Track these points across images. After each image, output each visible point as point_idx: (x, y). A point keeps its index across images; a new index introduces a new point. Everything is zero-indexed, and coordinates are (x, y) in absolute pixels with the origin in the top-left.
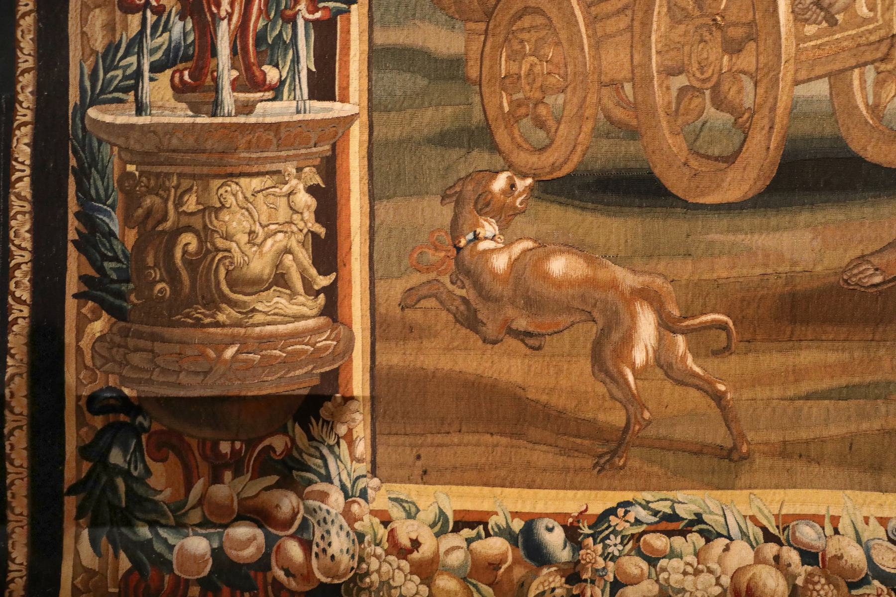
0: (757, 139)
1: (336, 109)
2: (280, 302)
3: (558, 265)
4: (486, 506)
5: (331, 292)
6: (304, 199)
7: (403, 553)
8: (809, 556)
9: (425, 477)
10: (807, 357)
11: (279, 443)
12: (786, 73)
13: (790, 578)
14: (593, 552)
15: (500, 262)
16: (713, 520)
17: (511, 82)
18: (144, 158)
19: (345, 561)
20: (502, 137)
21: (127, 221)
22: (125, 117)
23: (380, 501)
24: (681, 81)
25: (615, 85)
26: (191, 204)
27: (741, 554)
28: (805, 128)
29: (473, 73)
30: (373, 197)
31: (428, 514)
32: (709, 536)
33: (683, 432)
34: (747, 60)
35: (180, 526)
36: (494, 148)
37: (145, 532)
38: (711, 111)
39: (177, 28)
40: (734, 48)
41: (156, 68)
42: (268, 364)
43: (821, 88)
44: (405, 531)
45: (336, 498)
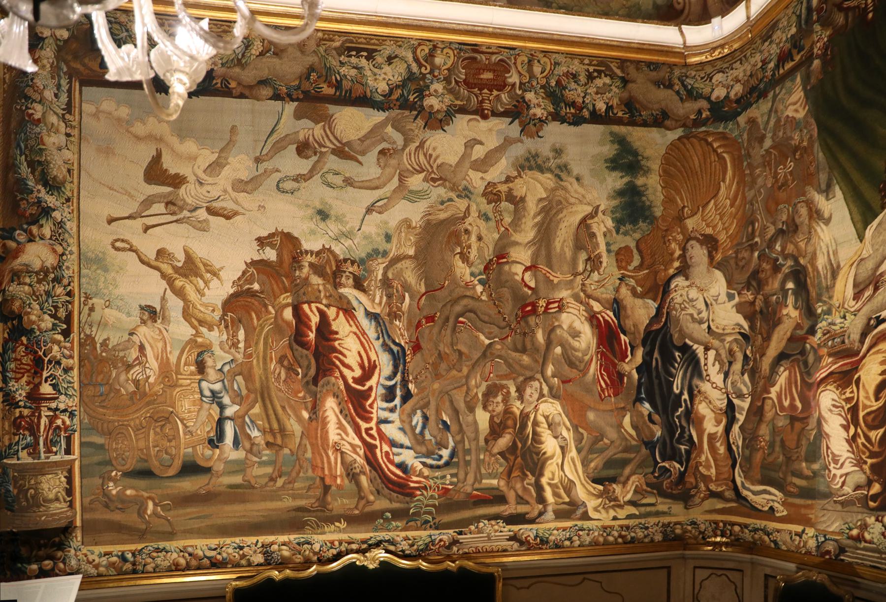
0: (176, 461)
1: (71, 457)
2: (58, 505)
3: (128, 492)
4: (112, 550)
5: (71, 501)
6: (63, 479)
7: (90, 563)
8: (190, 555)
9: (96, 544)
10: (189, 510)
11: (57, 539)
12: (182, 446)
13: (186, 560)
14: (139, 558)
15: (114, 492)
16: (168, 548)
17: (116, 449)
18: (19, 471)
19: (75, 566)
20: (114, 462)
21: (15, 487)
22: (14, 461)
23: (84, 551)
24: (158, 449)
25: (141, 450)
26: (33, 482)
27: (175, 555)
28: (187, 459)
29: (107, 447)
30: (82, 478)
31: (97, 553)
32: (167, 552)
33: (161, 529)
34: (173, 443)
35: (29, 563)
36: (112, 465)
37: (19, 565)
38: (165, 455)
39: (29, 439)
40: (170, 441)
41: (23, 449)
42: (54, 520)
43: (190, 450)
44: (91, 558)
45: (73, 551)
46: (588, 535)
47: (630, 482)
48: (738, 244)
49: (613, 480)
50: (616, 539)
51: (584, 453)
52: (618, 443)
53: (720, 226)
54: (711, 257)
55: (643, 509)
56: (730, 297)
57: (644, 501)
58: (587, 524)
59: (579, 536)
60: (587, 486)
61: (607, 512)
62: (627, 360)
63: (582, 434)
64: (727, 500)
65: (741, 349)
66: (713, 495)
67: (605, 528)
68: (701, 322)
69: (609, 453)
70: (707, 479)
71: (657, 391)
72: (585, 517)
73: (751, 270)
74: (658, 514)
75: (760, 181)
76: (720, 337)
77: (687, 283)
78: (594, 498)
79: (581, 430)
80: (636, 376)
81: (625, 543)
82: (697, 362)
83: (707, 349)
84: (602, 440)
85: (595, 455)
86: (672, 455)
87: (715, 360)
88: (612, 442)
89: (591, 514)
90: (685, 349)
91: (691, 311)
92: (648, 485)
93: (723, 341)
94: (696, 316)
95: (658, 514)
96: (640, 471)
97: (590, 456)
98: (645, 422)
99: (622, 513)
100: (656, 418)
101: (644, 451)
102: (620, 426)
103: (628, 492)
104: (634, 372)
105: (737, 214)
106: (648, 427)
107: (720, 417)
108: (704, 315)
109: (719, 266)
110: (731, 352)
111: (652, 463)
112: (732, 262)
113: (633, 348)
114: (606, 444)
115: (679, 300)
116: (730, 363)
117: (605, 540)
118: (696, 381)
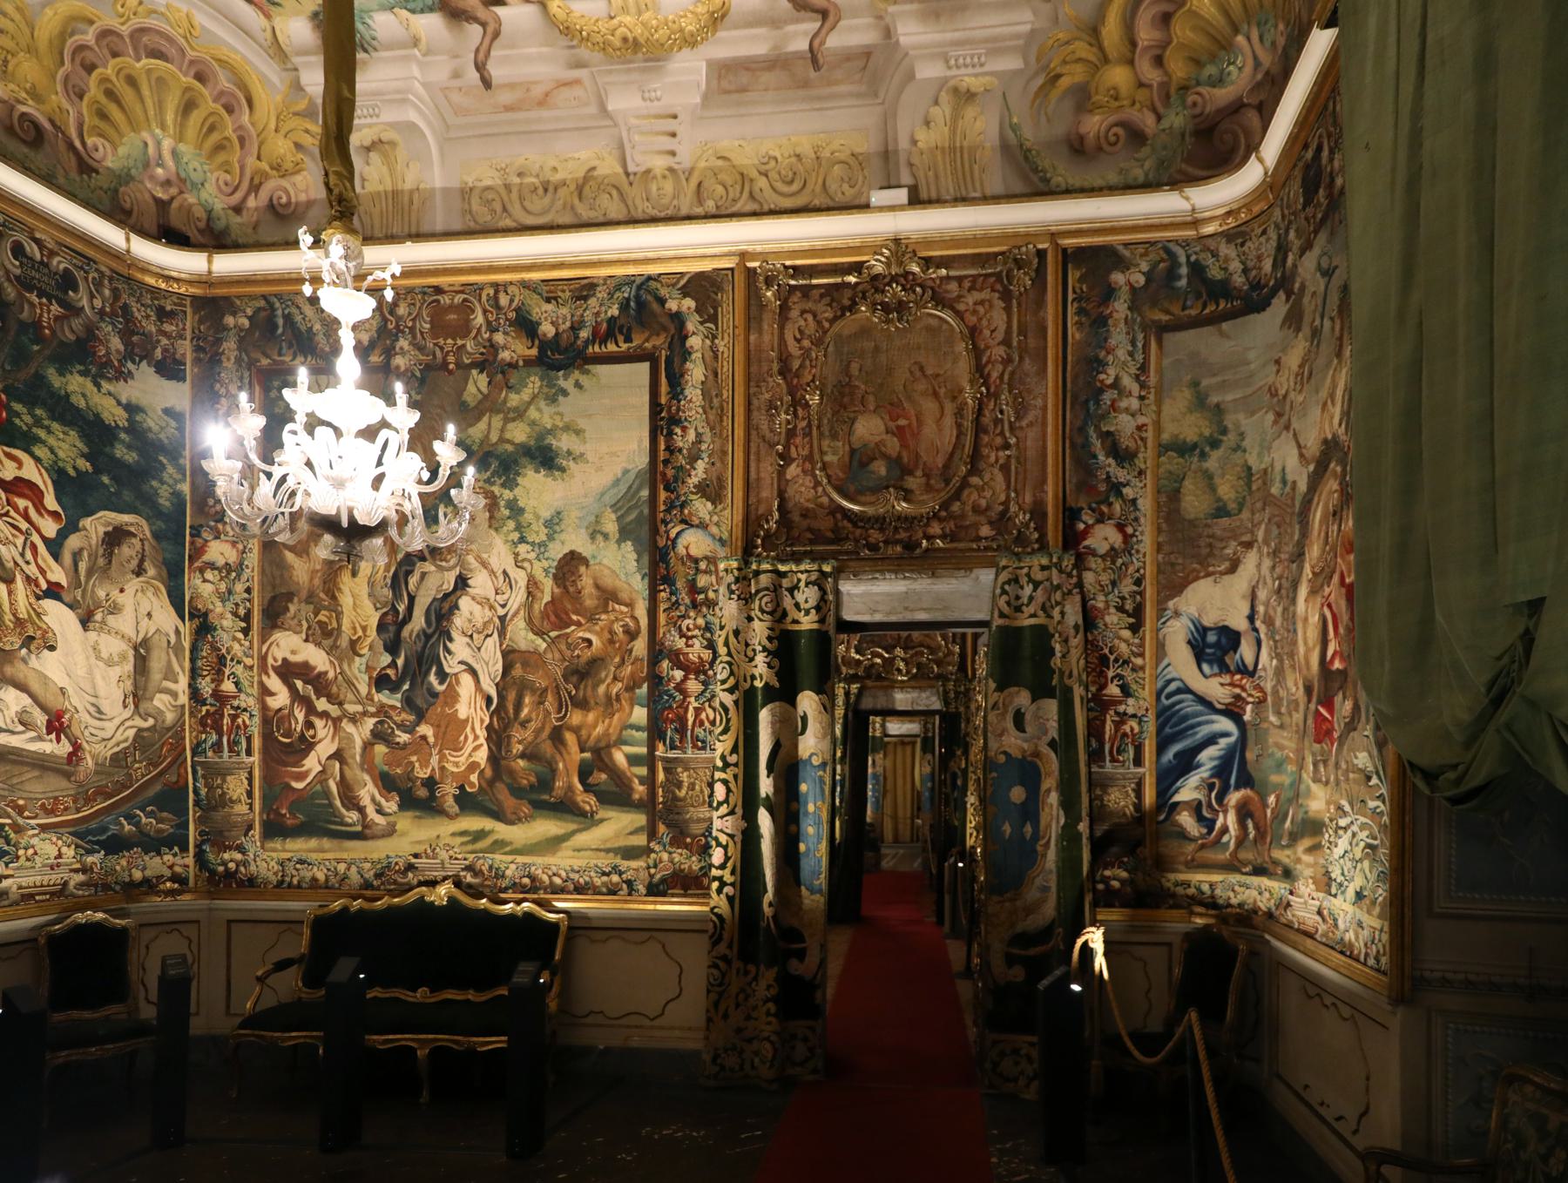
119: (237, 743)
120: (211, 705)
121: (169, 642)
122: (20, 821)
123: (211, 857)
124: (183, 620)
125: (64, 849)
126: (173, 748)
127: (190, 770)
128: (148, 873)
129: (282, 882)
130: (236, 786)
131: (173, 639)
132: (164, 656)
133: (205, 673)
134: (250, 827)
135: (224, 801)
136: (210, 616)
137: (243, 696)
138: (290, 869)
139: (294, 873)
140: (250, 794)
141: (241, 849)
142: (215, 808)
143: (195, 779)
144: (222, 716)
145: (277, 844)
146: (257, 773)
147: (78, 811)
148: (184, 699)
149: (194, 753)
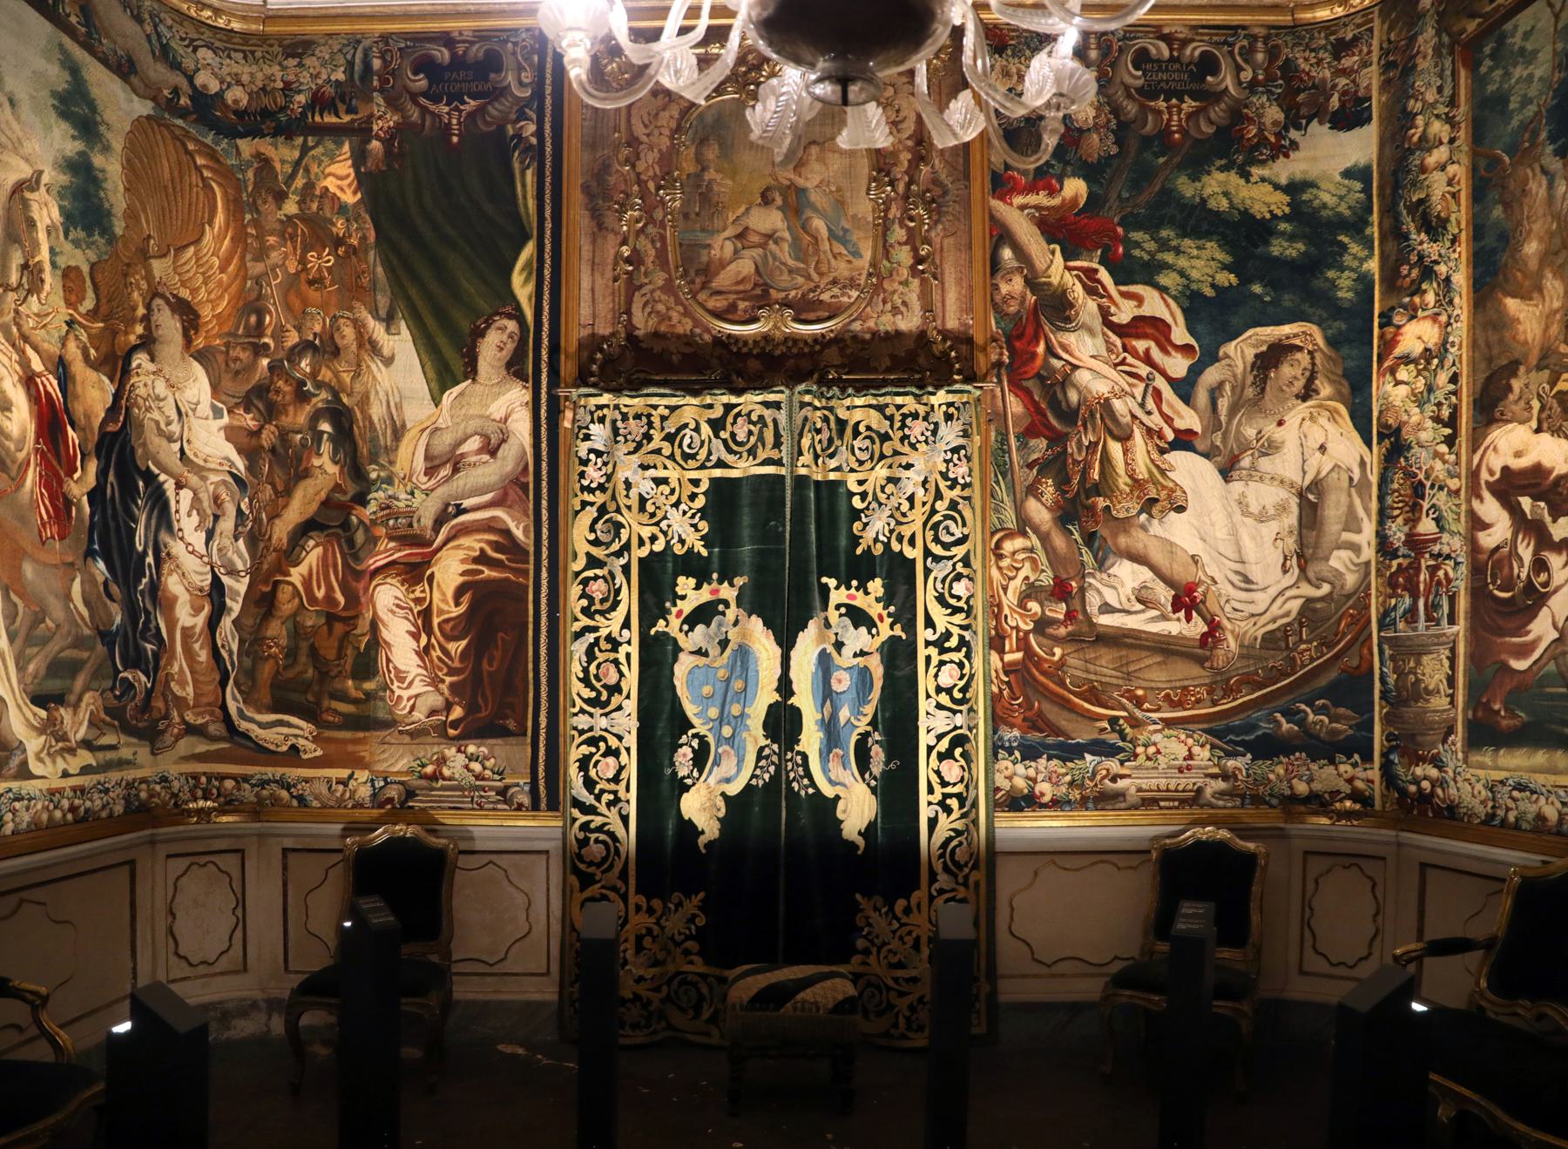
46: (28, 809)
47: (83, 705)
48: (229, 334)
49: (59, 699)
50: (64, 815)
51: (19, 642)
52: (65, 628)
53: (202, 294)
54: (188, 341)
55: (100, 755)
56: (217, 414)
57: (105, 741)
58: (29, 787)
59: (14, 812)
60: (25, 709)
61: (54, 762)
62: (76, 476)
63: (15, 605)
64: (214, 739)
65: (233, 499)
66: (191, 730)
67: (52, 792)
68: (170, 439)
69: (53, 648)
70: (181, 703)
71: (114, 543)
72: (24, 773)
73: (253, 382)
74: (122, 764)
75: (275, 256)
76: (200, 471)
77: (151, 367)
78: (34, 734)
79: (14, 597)
80: (87, 509)
81: (76, 821)
82: (166, 504)
83: (179, 486)
84: (43, 621)
85: (35, 650)
86: (135, 660)
87: (192, 507)
88: (58, 626)
89: (35, 767)
90: (150, 478)
91: (156, 415)
92: (107, 711)
93: (204, 479)
94: (163, 426)
95: (122, 764)
96: (95, 685)
97: (28, 651)
98: (99, 597)
99: (74, 764)
100: (115, 589)
101: (100, 648)
102: (68, 597)
103: (81, 724)
104: (85, 498)
105: (229, 286)
106: (105, 605)
107: (198, 602)
108: (175, 428)
109: (202, 357)
110: (216, 500)
111: (111, 671)
112: (221, 358)
113: (83, 456)
114: (49, 629)
115: (141, 391)
116: (216, 518)
117: (50, 818)
118: (164, 536)
119: (1436, 606)
120: (1404, 556)
121: (1351, 479)
122: (1139, 714)
123: (1400, 770)
124: (1369, 444)
125: (1196, 750)
126: (1354, 621)
127: (1376, 650)
128: (1316, 786)
129: (1493, 816)
130: (1433, 671)
131: (1356, 476)
132: (1344, 499)
133: (1396, 512)
134: (1450, 730)
135: (1418, 693)
136: (1404, 431)
137: (1446, 537)
138: (1504, 800)
139: (1511, 804)
140: (1451, 681)
141: (1437, 762)
142: (1404, 702)
143: (1382, 663)
144: (1418, 570)
145: (1485, 757)
146: (1461, 649)
147: (1215, 703)
148: (1369, 553)
149: (1382, 626)
